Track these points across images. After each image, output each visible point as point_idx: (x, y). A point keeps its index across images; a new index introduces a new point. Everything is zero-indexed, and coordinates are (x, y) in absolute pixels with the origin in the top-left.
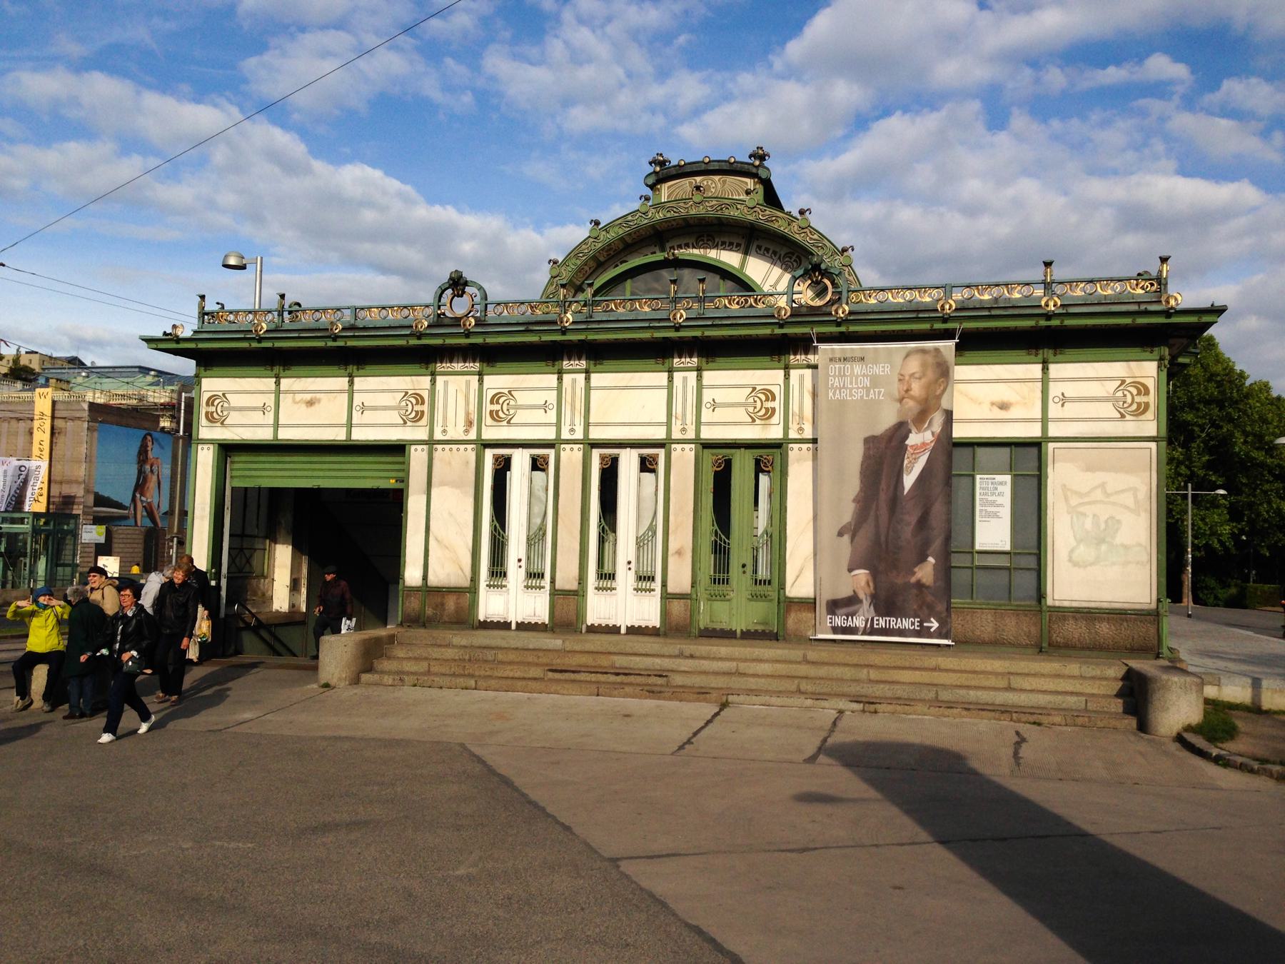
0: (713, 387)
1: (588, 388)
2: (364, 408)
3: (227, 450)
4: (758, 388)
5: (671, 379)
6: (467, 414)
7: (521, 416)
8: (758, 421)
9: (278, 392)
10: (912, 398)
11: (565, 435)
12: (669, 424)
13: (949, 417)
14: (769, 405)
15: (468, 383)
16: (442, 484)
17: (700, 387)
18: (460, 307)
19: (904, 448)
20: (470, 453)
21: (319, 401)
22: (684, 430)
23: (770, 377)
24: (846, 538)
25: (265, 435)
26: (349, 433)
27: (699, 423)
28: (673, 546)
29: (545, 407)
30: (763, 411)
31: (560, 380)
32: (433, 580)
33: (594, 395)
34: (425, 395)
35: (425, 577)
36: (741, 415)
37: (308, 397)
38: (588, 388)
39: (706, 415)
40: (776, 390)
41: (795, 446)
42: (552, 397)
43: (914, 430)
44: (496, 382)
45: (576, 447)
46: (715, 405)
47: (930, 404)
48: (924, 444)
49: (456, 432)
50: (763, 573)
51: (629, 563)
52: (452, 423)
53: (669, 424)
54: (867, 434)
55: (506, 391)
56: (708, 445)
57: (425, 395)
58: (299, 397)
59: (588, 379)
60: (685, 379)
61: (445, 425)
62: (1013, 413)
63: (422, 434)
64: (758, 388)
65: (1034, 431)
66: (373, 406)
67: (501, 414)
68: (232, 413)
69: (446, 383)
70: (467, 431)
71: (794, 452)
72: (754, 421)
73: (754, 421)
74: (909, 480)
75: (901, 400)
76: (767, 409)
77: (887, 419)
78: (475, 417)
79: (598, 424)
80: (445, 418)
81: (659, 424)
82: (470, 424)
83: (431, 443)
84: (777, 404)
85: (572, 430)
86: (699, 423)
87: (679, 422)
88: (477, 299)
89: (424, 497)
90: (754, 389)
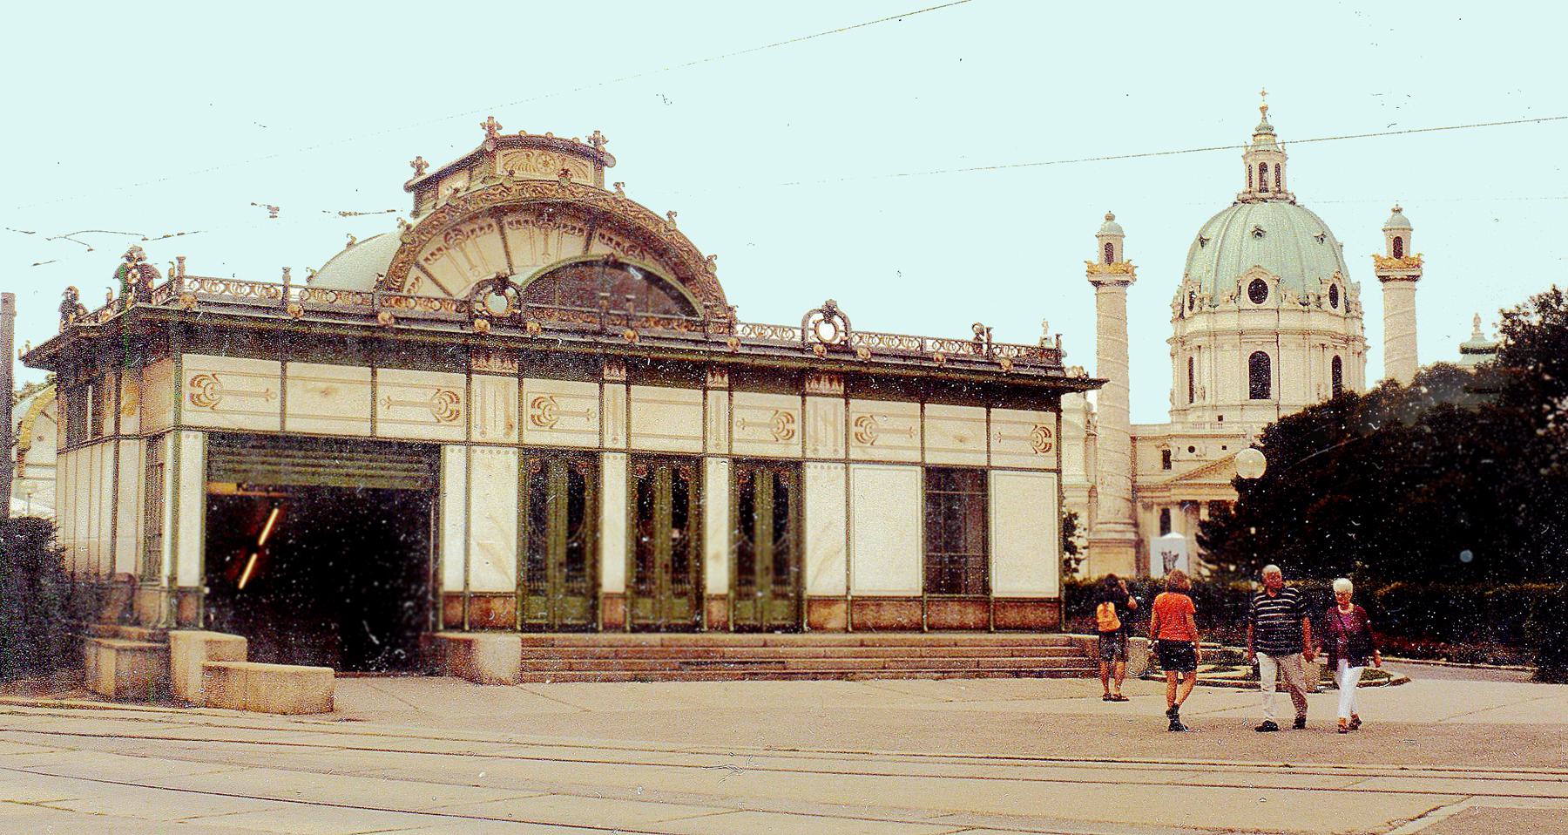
1: (628, 400)
2: (390, 403)
3: (222, 443)
6: (508, 417)
9: (284, 378)
14: (790, 426)
21: (336, 390)
23: (790, 402)
25: (271, 425)
26: (373, 429)
32: (476, 586)
33: (633, 404)
34: (461, 394)
35: (467, 584)
37: (323, 385)
42: (594, 405)
45: (619, 455)
46: (744, 425)
49: (496, 433)
56: (736, 461)
58: (311, 385)
60: (718, 398)
61: (483, 425)
62: (969, 446)
65: (979, 461)
66: (405, 404)
68: (228, 398)
70: (507, 434)
79: (638, 435)
80: (483, 419)
81: (695, 438)
84: (797, 427)
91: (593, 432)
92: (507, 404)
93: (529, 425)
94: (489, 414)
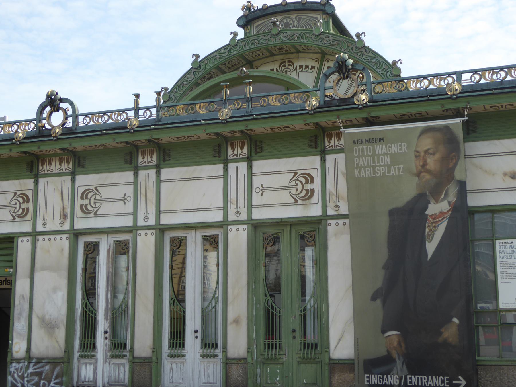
0: (261, 174)
1: (159, 181)
4: (299, 172)
5: (226, 169)
6: (63, 209)
7: (105, 208)
8: (300, 202)
10: (428, 172)
11: (141, 222)
12: (225, 209)
13: (463, 189)
14: (309, 186)
15: (63, 182)
16: (43, 269)
17: (250, 174)
18: (57, 119)
19: (424, 218)
20: (64, 242)
22: (238, 212)
23: (310, 163)
24: (379, 302)
27: (250, 206)
28: (231, 317)
29: (124, 199)
30: (304, 193)
31: (136, 175)
34: (30, 194)
36: (285, 197)
38: (159, 181)
39: (256, 199)
40: (314, 173)
41: (333, 222)
42: (129, 190)
43: (432, 201)
44: (84, 181)
45: (149, 232)
46: (263, 190)
47: (445, 176)
48: (442, 213)
49: (54, 225)
50: (311, 337)
51: (196, 331)
52: (50, 217)
53: (225, 209)
54: (391, 207)
55: (93, 188)
57: (30, 194)
59: (158, 174)
61: (45, 219)
63: (27, 228)
64: (299, 172)
67: (89, 207)
69: (46, 184)
70: (62, 223)
71: (333, 228)
72: (296, 201)
73: (296, 201)
74: (431, 247)
75: (418, 175)
76: (307, 191)
77: (408, 190)
78: (68, 211)
80: (45, 213)
81: (217, 209)
82: (64, 216)
83: (34, 234)
84: (316, 186)
85: (146, 218)
86: (250, 206)
87: (234, 206)
88: (70, 113)
89: (28, 281)
90: (296, 173)
91: (128, 214)
92: (63, 199)
93: (79, 213)
94: (50, 210)
